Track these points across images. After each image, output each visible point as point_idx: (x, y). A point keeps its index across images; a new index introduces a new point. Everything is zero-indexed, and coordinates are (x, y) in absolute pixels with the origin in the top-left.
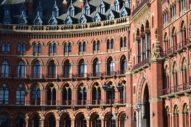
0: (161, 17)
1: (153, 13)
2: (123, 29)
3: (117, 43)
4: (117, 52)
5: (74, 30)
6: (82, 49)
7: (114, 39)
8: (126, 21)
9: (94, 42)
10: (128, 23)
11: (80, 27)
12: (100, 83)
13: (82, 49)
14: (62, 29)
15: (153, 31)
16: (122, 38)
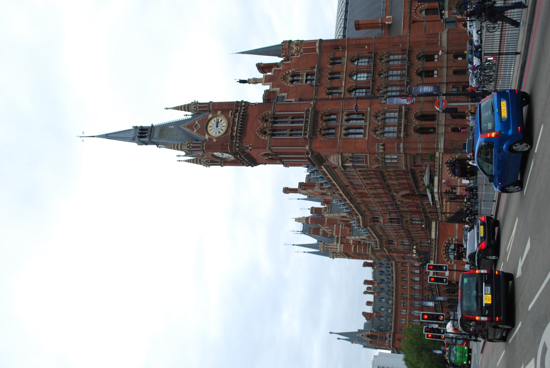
0: (397, 251)
1: (395, 254)
2: (396, 264)
3: (403, 268)
4: (408, 268)
5: (394, 291)
6: (405, 287)
7: (401, 269)
8: (392, 263)
9: (402, 280)
10: (393, 262)
11: (393, 287)
12: (425, 279)
13: (405, 287)
14: (393, 297)
15: (402, 255)
16: (402, 266)
